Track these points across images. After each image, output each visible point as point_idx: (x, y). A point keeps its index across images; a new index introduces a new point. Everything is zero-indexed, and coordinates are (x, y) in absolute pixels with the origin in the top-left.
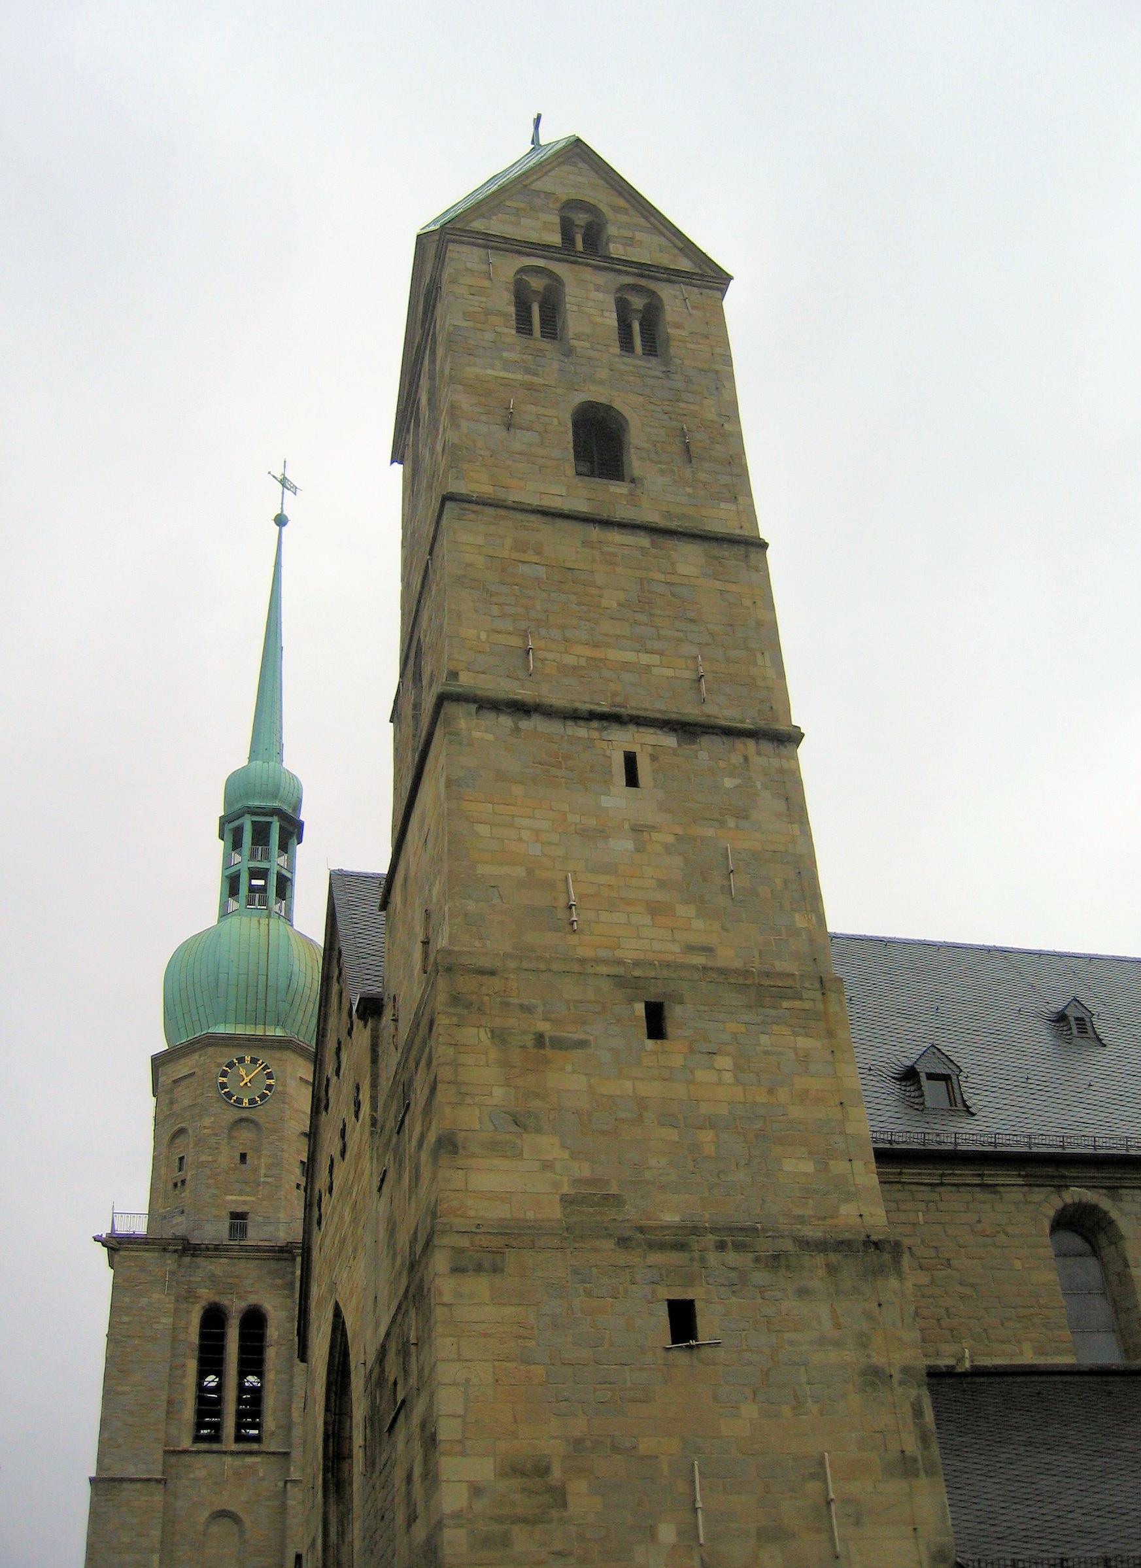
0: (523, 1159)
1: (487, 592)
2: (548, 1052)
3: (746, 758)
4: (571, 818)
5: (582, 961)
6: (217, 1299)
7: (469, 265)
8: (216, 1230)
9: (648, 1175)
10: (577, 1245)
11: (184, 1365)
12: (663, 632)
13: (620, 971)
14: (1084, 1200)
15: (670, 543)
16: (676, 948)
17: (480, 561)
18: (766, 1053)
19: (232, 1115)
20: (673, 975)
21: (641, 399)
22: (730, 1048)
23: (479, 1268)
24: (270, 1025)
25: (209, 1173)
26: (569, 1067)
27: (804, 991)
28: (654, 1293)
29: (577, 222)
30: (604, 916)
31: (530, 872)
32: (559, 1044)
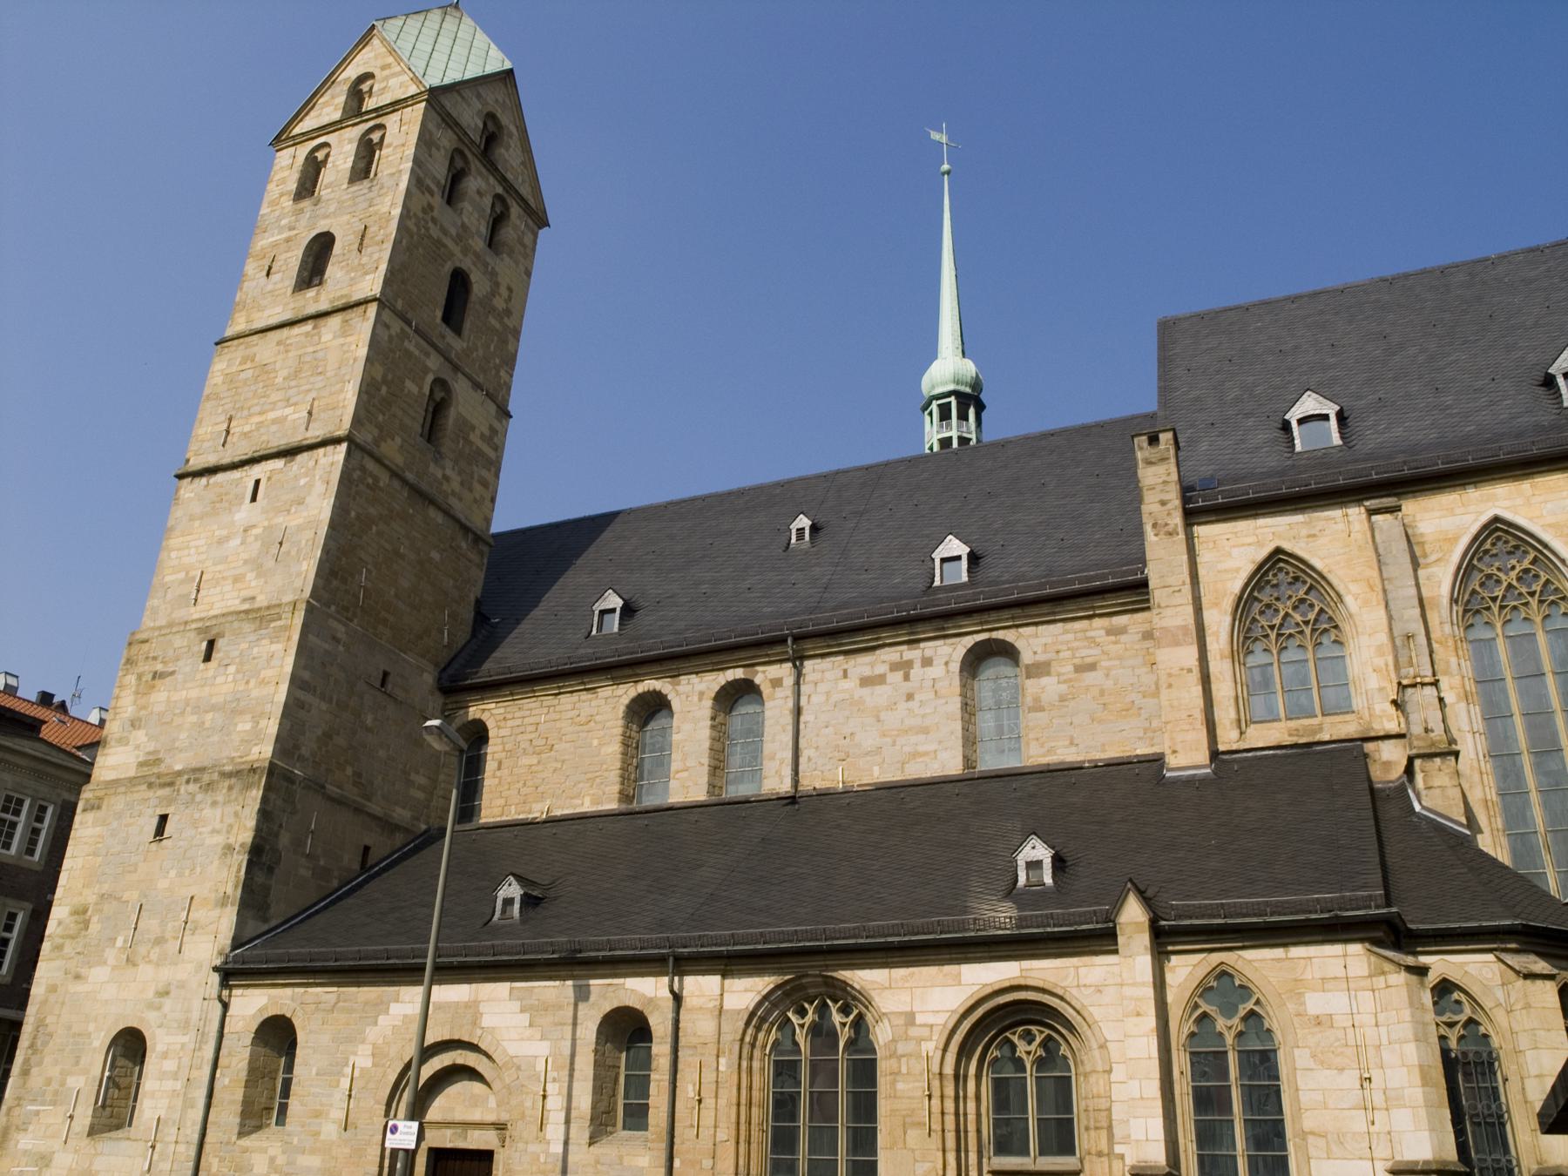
14: (651, 689)
16: (237, 602)
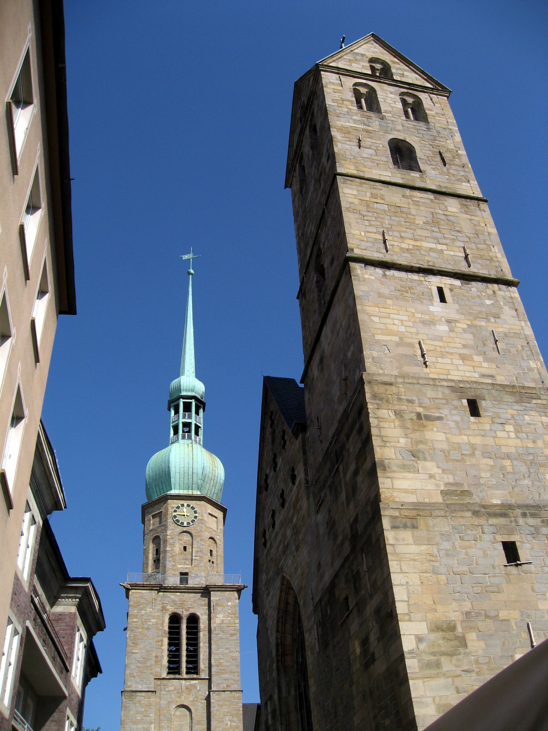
0: (419, 473)
1: (361, 215)
2: (424, 422)
3: (494, 292)
4: (416, 315)
5: (434, 379)
6: (176, 611)
7: (331, 81)
8: (173, 580)
9: (482, 481)
10: (453, 515)
11: (162, 640)
12: (446, 236)
13: (453, 384)
15: (442, 198)
16: (477, 375)
17: (356, 201)
18: (528, 424)
19: (180, 529)
20: (479, 387)
21: (418, 139)
22: (512, 422)
23: (405, 527)
24: (194, 490)
25: (170, 555)
26: (435, 429)
27: (541, 396)
28: (494, 538)
29: (377, 68)
30: (440, 360)
31: (401, 339)
32: (428, 418)
